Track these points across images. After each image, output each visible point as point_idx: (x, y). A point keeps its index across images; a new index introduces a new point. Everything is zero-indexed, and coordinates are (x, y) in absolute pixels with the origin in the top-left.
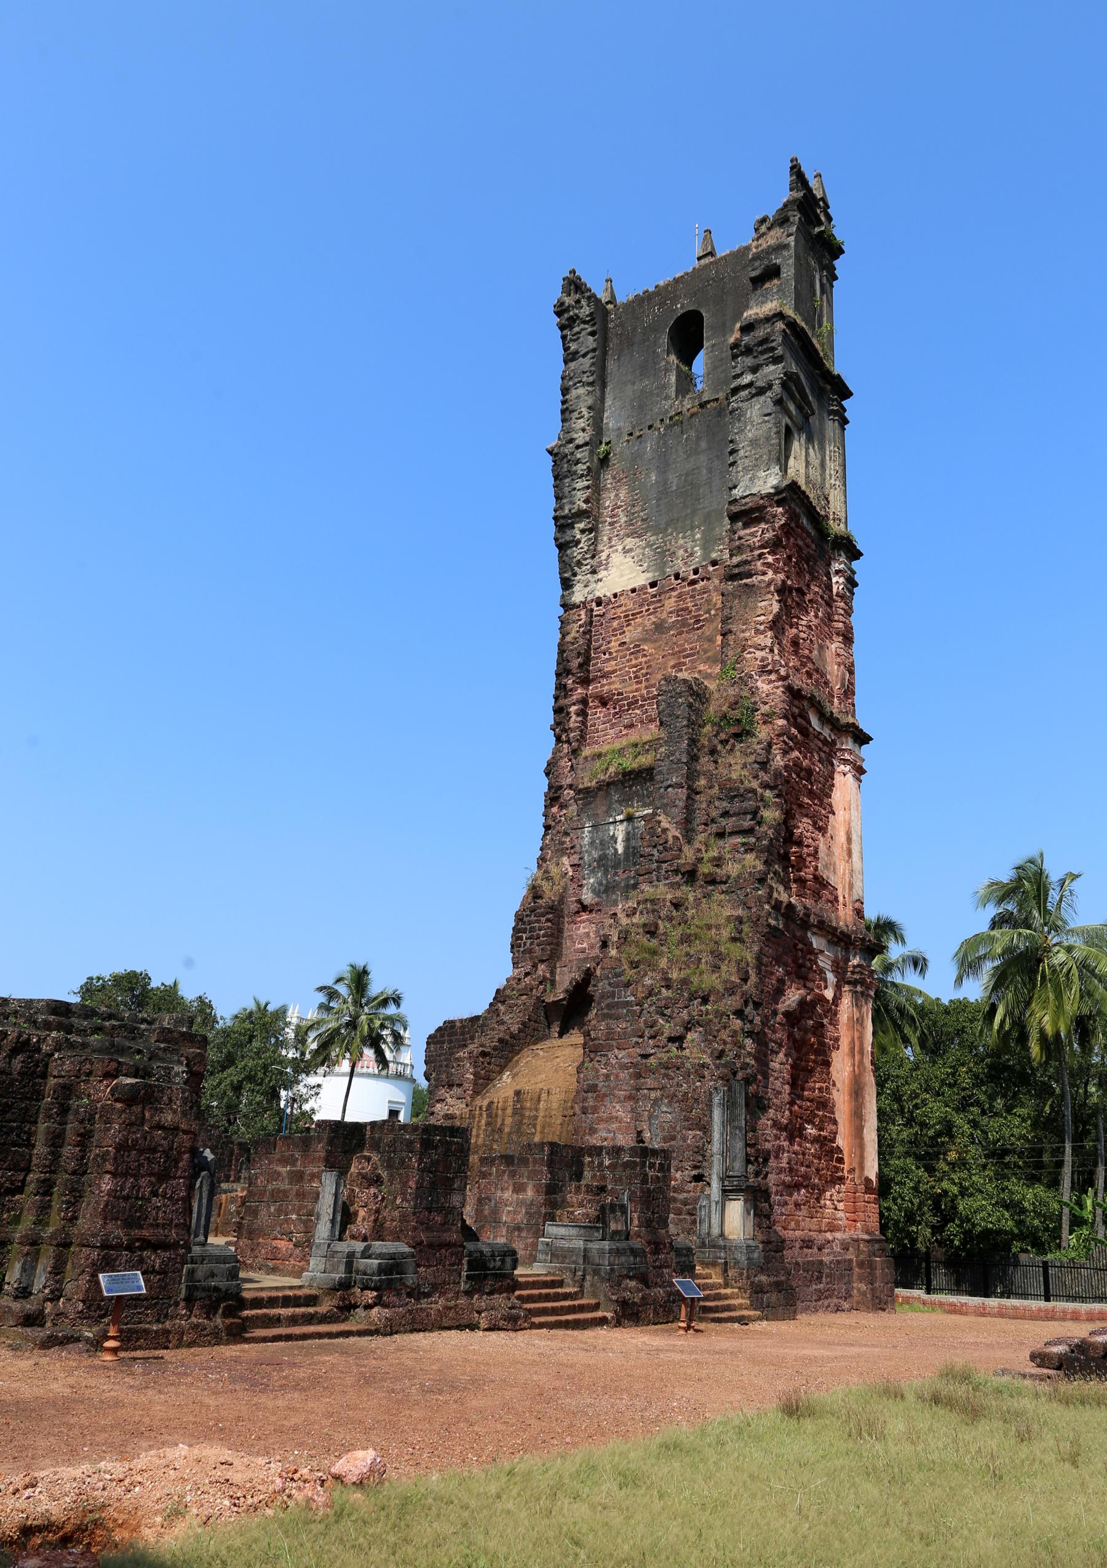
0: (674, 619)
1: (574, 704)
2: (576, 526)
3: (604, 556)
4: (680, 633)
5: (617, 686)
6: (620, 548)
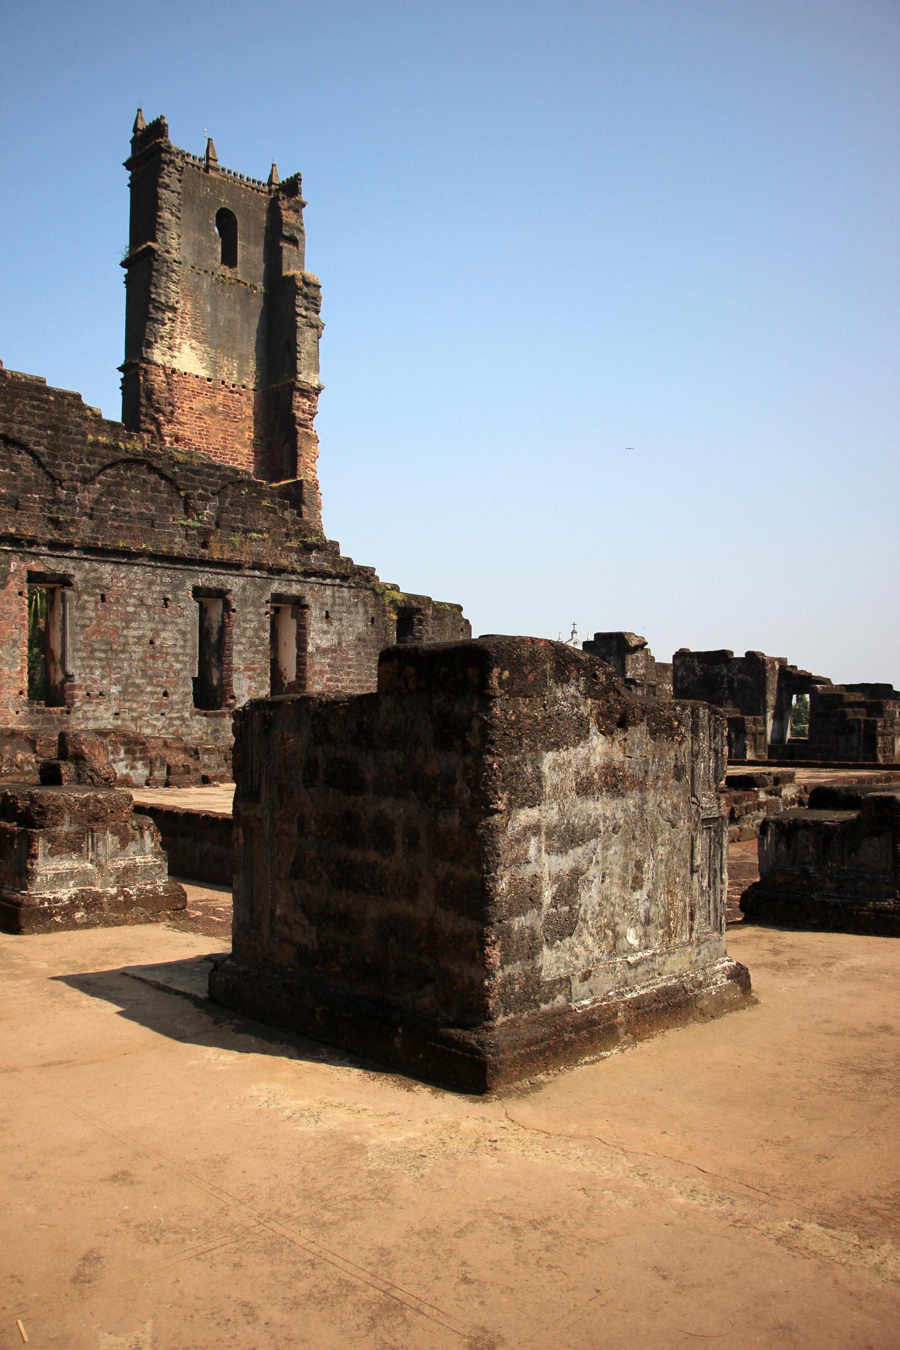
0: (221, 409)
1: (168, 436)
2: (167, 313)
3: (178, 341)
4: (226, 420)
5: (187, 434)
6: (188, 343)
